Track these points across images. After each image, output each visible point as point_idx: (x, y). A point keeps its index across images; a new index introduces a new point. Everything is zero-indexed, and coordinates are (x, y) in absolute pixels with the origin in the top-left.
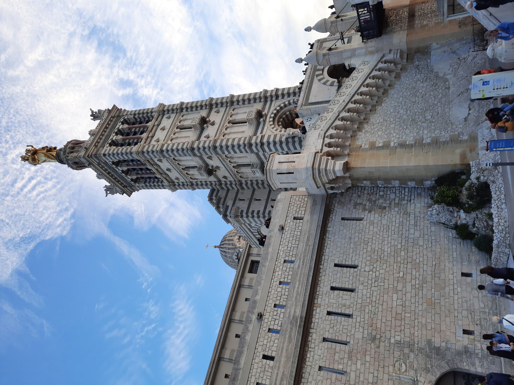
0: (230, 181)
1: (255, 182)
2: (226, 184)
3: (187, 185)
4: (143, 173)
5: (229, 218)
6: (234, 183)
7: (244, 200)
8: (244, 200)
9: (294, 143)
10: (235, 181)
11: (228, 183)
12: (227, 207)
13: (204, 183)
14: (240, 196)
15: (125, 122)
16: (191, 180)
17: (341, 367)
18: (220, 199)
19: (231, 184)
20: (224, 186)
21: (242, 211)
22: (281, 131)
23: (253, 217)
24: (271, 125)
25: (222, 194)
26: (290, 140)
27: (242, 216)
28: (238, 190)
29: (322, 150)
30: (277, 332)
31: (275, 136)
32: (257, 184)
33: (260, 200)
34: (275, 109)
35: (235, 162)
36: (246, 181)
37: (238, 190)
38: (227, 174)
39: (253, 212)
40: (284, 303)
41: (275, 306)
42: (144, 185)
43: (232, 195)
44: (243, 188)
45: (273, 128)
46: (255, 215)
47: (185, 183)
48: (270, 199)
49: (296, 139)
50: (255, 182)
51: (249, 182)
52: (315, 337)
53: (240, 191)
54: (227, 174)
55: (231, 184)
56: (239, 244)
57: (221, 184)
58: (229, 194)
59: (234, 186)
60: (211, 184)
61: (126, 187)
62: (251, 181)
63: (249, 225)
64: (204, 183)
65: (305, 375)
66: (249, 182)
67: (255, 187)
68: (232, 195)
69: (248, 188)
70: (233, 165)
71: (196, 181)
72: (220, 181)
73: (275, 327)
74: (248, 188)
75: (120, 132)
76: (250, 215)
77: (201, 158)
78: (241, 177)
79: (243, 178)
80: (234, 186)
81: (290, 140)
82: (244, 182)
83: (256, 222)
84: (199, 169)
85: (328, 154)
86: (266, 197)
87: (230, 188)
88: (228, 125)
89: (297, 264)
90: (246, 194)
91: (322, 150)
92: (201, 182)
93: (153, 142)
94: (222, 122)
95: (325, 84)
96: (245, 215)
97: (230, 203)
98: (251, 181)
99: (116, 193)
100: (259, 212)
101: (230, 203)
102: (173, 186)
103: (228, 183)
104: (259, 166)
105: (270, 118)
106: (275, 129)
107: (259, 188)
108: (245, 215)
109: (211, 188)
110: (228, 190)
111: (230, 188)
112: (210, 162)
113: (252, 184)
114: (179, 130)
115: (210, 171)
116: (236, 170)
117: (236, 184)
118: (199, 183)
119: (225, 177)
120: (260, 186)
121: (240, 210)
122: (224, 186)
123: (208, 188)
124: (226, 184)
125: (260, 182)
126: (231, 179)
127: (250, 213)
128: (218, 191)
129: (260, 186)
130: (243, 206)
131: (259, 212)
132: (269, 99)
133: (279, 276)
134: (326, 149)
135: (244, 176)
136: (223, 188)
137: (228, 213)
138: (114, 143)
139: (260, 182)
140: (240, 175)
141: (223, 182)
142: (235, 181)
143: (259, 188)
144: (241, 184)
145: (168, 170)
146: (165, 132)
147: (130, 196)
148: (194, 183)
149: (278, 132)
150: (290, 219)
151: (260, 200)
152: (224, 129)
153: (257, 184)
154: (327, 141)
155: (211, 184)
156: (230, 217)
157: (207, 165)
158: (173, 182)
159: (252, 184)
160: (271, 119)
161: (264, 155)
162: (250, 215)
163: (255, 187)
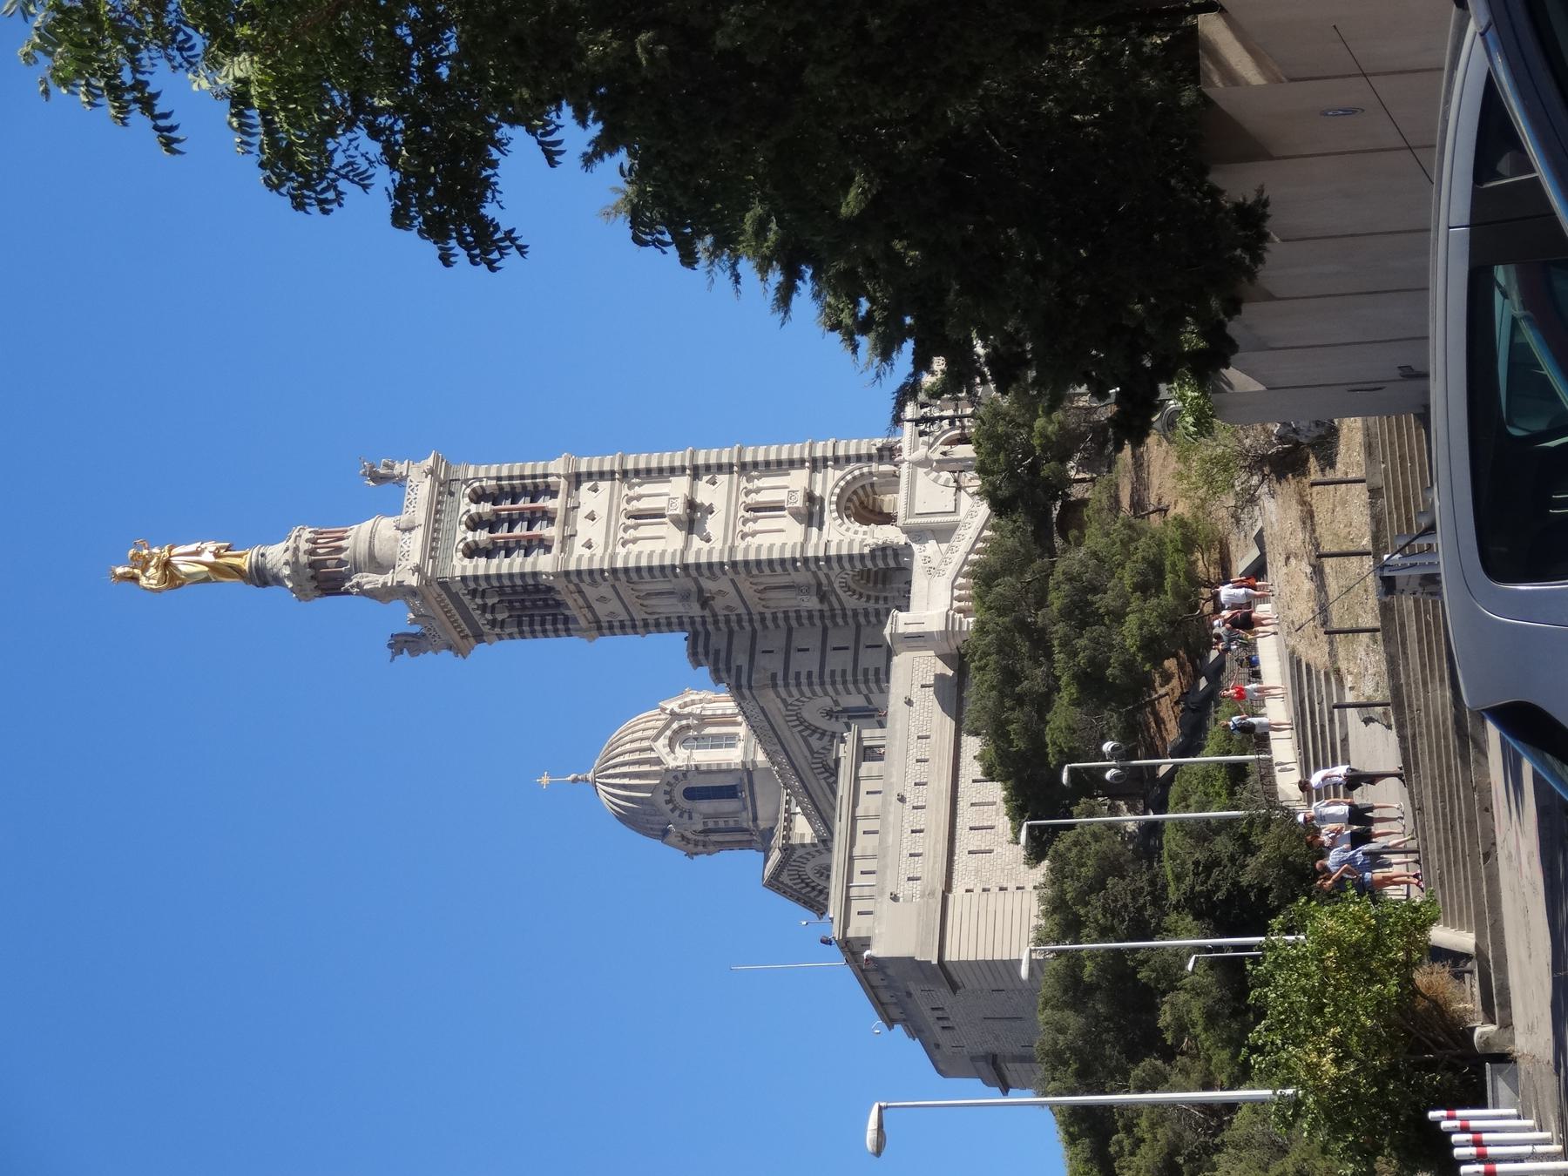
0: (738, 615)
1: (792, 615)
2: (728, 621)
3: (634, 627)
4: (524, 608)
5: (746, 692)
6: (745, 617)
7: (772, 652)
8: (772, 652)
9: (885, 557)
10: (750, 614)
11: (733, 618)
12: (739, 668)
13: (675, 620)
14: (759, 647)
15: (478, 497)
16: (646, 616)
17: (989, 823)
18: (717, 652)
19: (740, 620)
20: (722, 625)
21: (774, 676)
22: (856, 532)
23: (798, 685)
24: (835, 519)
25: (719, 641)
26: (879, 553)
27: (775, 686)
28: (754, 631)
29: (951, 605)
30: (923, 807)
31: (851, 543)
32: (799, 617)
33: (808, 650)
34: (836, 485)
35: (761, 583)
36: (774, 614)
37: (754, 631)
38: (735, 601)
39: (798, 675)
40: (925, 780)
41: (916, 784)
42: (516, 630)
43: (741, 643)
44: (765, 627)
45: (840, 525)
46: (804, 680)
47: (628, 623)
48: (828, 648)
49: (889, 552)
50: (792, 615)
51: (780, 615)
52: (963, 805)
53: (759, 634)
54: (735, 601)
55: (740, 620)
56: (676, 759)
57: (716, 622)
58: (735, 642)
59: (746, 624)
60: (693, 622)
61: (466, 637)
62: (785, 612)
63: (784, 701)
64: (675, 620)
65: (957, 836)
66: (780, 615)
67: (794, 623)
68: (741, 643)
69: (777, 626)
70: (755, 587)
71: (656, 616)
72: (715, 615)
73: (920, 804)
74: (777, 626)
75: (475, 523)
76: (792, 681)
77: (696, 581)
78: (763, 606)
79: (768, 607)
80: (746, 624)
81: (879, 553)
82: (769, 616)
83: (802, 694)
84: (685, 597)
85: (960, 611)
86: (819, 644)
87: (736, 628)
88: (748, 515)
89: (933, 738)
90: (776, 640)
91: (951, 605)
92: (667, 618)
93: (578, 548)
94: (733, 508)
95: (935, 481)
96: (780, 682)
97: (741, 659)
98: (785, 612)
99: (425, 652)
100: (810, 674)
101: (741, 659)
102: (600, 627)
103: (733, 618)
104: (814, 589)
105: (830, 503)
106: (844, 527)
107: (800, 624)
108: (780, 682)
109: (690, 629)
110: (731, 633)
111: (736, 628)
112: (708, 585)
113: (787, 618)
114: (632, 522)
115: (705, 602)
116: (759, 595)
117: (751, 620)
118: (663, 621)
119: (728, 608)
120: (805, 621)
121: (769, 674)
122: (722, 625)
123: (683, 630)
124: (728, 621)
125: (804, 614)
126: (742, 610)
127: (787, 677)
128: (707, 634)
129: (805, 621)
130: (774, 664)
131: (810, 674)
132: (820, 464)
133: (915, 753)
134: (956, 604)
135: (771, 604)
136: (718, 629)
137: (744, 681)
138: (472, 551)
139: (804, 614)
140: (763, 603)
141: (721, 618)
142: (750, 614)
143: (800, 624)
144: (763, 619)
145: (602, 599)
146: (601, 524)
147: (465, 658)
148: (651, 622)
149: (850, 533)
150: (917, 687)
151: (808, 650)
152: (740, 523)
153: (799, 617)
154: (957, 593)
155: (693, 622)
156: (750, 688)
157: (700, 590)
158: (598, 622)
159: (787, 618)
160: (834, 507)
161: (827, 576)
162: (792, 681)
163: (794, 623)
